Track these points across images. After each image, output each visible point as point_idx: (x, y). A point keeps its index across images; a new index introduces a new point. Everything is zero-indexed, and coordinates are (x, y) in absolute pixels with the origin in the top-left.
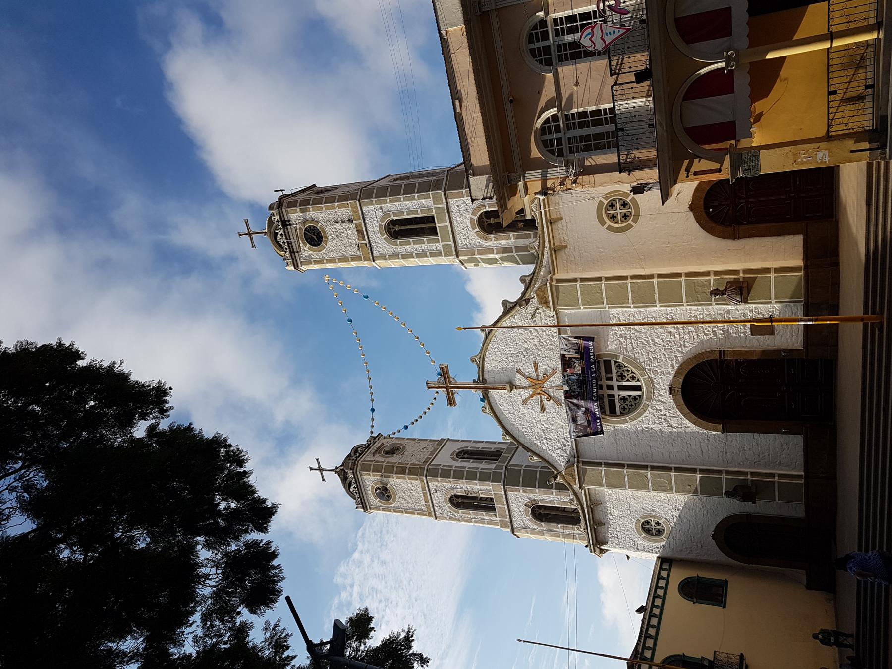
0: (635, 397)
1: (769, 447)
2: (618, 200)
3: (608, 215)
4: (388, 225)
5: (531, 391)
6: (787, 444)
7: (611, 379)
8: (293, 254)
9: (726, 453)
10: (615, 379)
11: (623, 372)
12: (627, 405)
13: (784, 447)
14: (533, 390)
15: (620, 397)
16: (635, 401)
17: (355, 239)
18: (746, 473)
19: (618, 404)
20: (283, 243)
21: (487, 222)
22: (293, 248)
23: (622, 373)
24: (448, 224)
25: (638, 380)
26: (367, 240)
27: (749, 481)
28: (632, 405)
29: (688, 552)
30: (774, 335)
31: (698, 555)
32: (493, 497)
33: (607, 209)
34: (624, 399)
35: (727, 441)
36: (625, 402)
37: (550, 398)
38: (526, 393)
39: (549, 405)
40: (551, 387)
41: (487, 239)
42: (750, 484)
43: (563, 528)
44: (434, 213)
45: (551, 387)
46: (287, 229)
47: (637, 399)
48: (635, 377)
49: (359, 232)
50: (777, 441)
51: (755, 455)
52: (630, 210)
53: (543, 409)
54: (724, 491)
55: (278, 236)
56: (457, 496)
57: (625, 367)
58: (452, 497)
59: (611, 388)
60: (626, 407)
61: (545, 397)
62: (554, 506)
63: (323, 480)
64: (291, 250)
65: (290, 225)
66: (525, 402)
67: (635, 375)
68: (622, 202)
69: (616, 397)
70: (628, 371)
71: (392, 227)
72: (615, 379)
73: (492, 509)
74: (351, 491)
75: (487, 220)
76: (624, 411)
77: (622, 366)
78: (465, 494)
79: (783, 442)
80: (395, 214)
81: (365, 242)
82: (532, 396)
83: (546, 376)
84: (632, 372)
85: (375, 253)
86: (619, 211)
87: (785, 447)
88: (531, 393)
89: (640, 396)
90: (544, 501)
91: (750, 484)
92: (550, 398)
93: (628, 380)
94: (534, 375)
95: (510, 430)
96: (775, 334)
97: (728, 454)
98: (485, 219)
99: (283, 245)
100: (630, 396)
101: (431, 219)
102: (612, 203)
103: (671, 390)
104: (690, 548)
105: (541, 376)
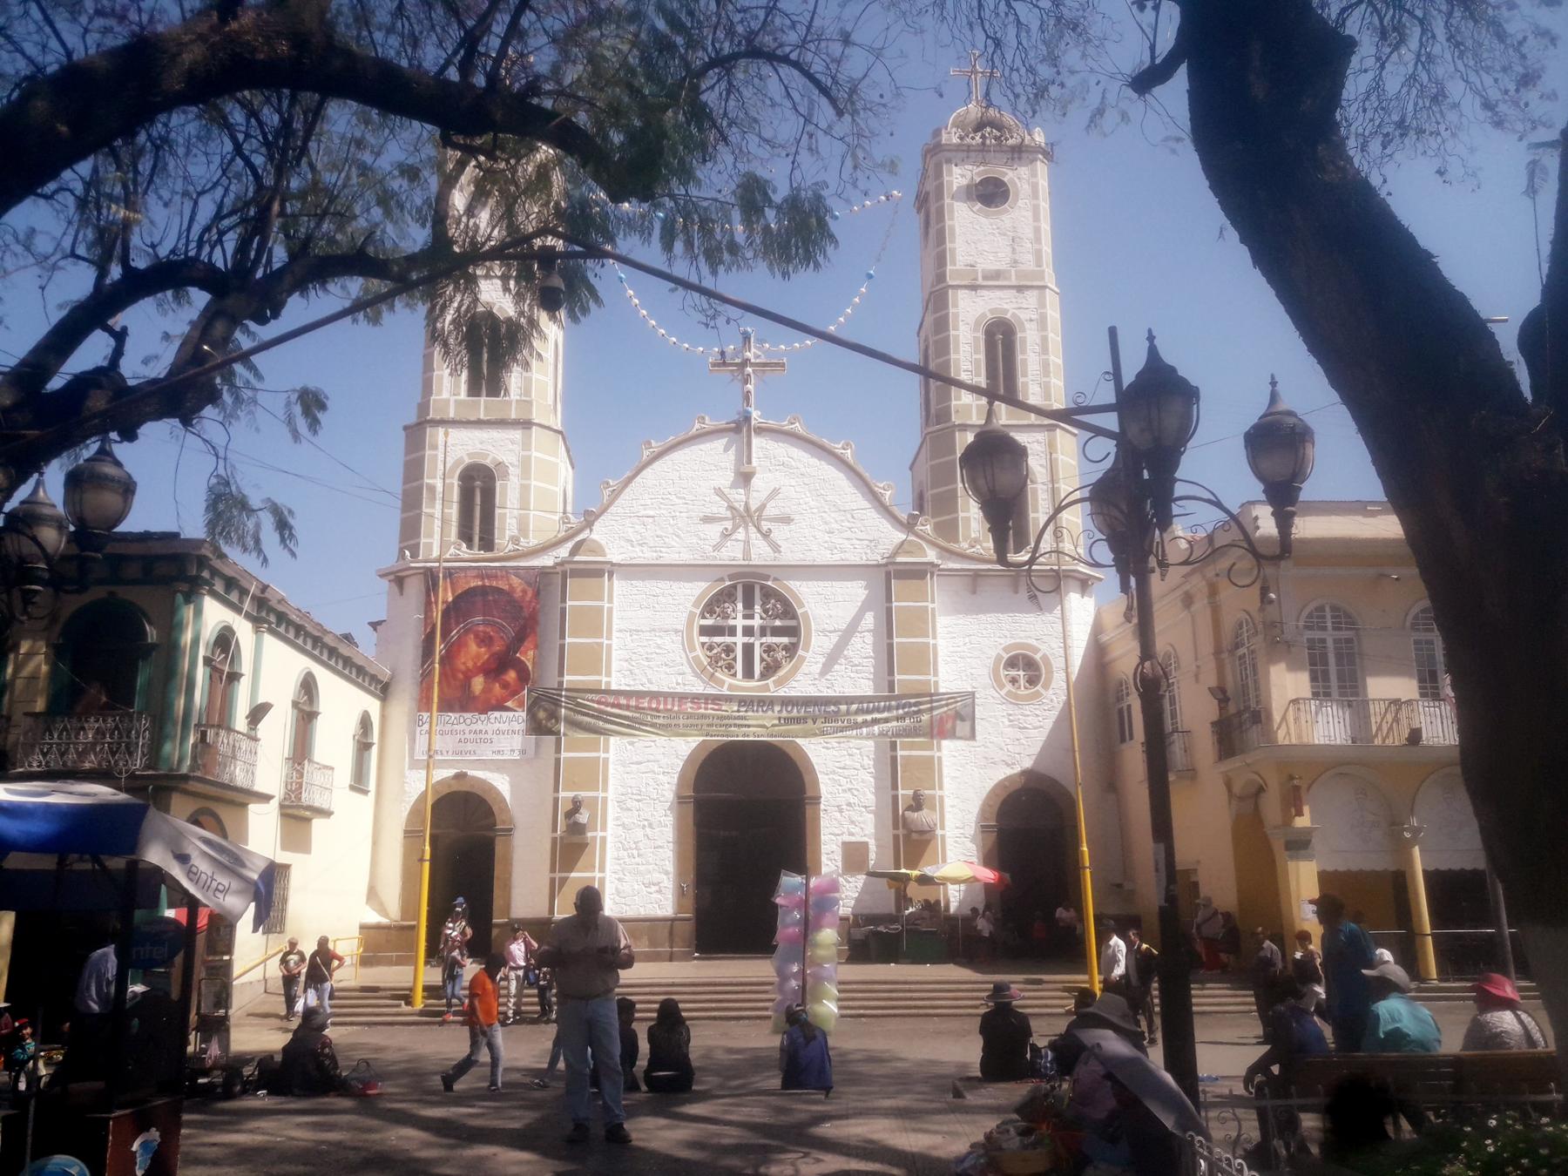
5: (742, 509)
6: (659, 892)
9: (638, 801)
14: (742, 509)
17: (987, 263)
26: (985, 283)
34: (729, 649)
37: (726, 535)
39: (714, 531)
45: (747, 542)
49: (997, 275)
53: (707, 520)
54: (583, 794)
59: (748, 631)
61: (729, 525)
65: (1013, 159)
66: (719, 492)
80: (1024, 340)
81: (980, 278)
83: (766, 535)
87: (654, 888)
88: (736, 505)
89: (734, 675)
90: (504, 487)
92: (726, 535)
93: (762, 660)
100: (735, 659)
105: (765, 526)
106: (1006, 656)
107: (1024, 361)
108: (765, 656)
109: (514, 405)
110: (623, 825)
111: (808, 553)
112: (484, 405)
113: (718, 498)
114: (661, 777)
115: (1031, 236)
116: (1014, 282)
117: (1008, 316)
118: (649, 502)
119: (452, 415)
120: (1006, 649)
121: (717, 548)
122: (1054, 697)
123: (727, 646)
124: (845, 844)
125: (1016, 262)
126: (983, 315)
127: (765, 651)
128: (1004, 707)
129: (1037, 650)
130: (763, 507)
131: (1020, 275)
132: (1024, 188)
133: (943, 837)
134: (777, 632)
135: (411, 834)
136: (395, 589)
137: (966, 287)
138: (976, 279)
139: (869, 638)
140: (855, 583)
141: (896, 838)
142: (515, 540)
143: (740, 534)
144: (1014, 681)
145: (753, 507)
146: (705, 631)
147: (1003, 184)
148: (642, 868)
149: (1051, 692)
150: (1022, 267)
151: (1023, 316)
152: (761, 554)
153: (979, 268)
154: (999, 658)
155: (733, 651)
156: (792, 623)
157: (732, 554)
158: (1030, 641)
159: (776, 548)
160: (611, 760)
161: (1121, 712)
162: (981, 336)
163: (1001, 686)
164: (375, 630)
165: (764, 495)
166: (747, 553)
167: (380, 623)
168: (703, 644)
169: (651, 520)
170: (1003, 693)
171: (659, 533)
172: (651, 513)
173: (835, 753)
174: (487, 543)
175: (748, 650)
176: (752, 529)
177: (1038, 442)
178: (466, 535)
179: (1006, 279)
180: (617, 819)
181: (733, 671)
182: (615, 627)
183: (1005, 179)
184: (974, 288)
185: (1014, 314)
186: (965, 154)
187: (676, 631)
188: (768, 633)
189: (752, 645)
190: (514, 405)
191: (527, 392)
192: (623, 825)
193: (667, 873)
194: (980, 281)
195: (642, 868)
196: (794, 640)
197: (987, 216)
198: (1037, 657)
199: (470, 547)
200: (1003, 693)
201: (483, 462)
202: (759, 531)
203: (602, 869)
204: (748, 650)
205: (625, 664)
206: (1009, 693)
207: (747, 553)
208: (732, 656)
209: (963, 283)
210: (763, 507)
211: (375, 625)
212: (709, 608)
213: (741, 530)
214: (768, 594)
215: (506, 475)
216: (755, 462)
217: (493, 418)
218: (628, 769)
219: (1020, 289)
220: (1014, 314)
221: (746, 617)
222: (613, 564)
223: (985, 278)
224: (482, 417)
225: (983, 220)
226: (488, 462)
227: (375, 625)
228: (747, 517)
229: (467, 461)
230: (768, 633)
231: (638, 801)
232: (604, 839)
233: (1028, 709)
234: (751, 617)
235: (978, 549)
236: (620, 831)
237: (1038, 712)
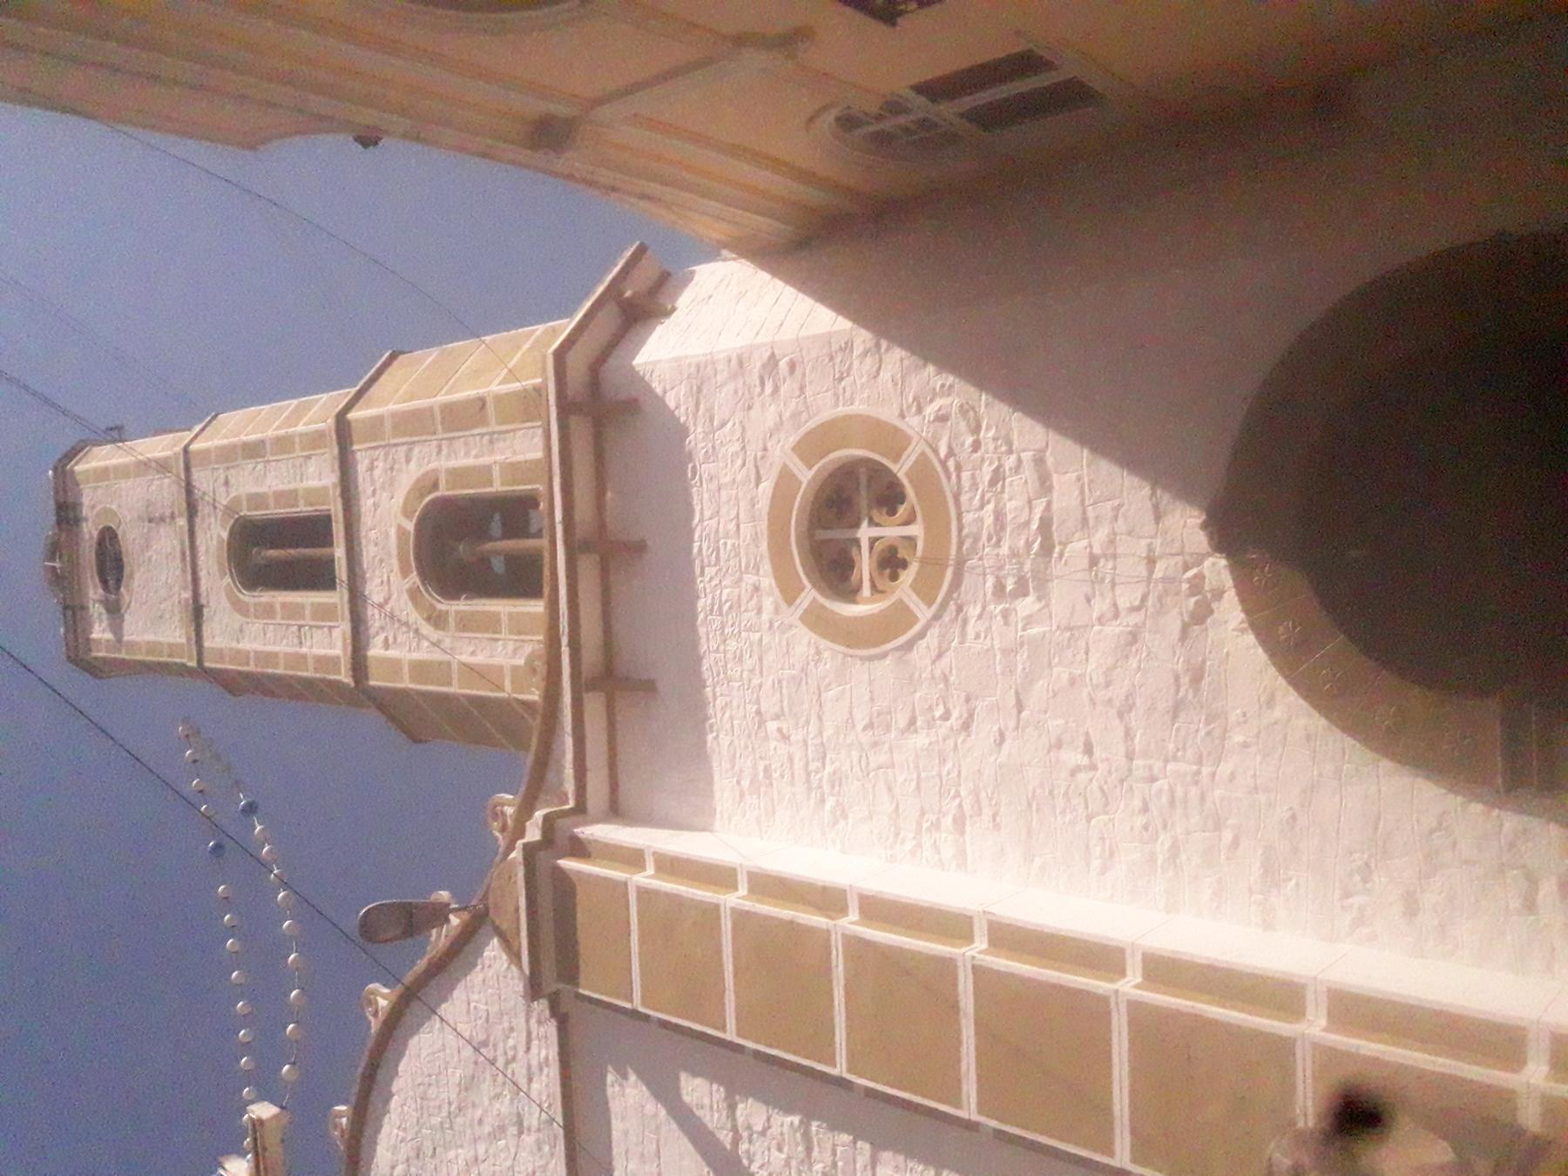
106: (810, 595)
120: (789, 593)
122: (930, 410)
128: (973, 611)
129: (786, 479)
139: (751, 1112)
140: (615, 1106)
144: (891, 562)
149: (912, 424)
154: (817, 621)
158: (764, 505)
170: (924, 613)
197: (131, 576)
198: (806, 476)
200: (924, 613)
206: (926, 590)
225: (137, 582)
233: (977, 516)
237: (986, 473)
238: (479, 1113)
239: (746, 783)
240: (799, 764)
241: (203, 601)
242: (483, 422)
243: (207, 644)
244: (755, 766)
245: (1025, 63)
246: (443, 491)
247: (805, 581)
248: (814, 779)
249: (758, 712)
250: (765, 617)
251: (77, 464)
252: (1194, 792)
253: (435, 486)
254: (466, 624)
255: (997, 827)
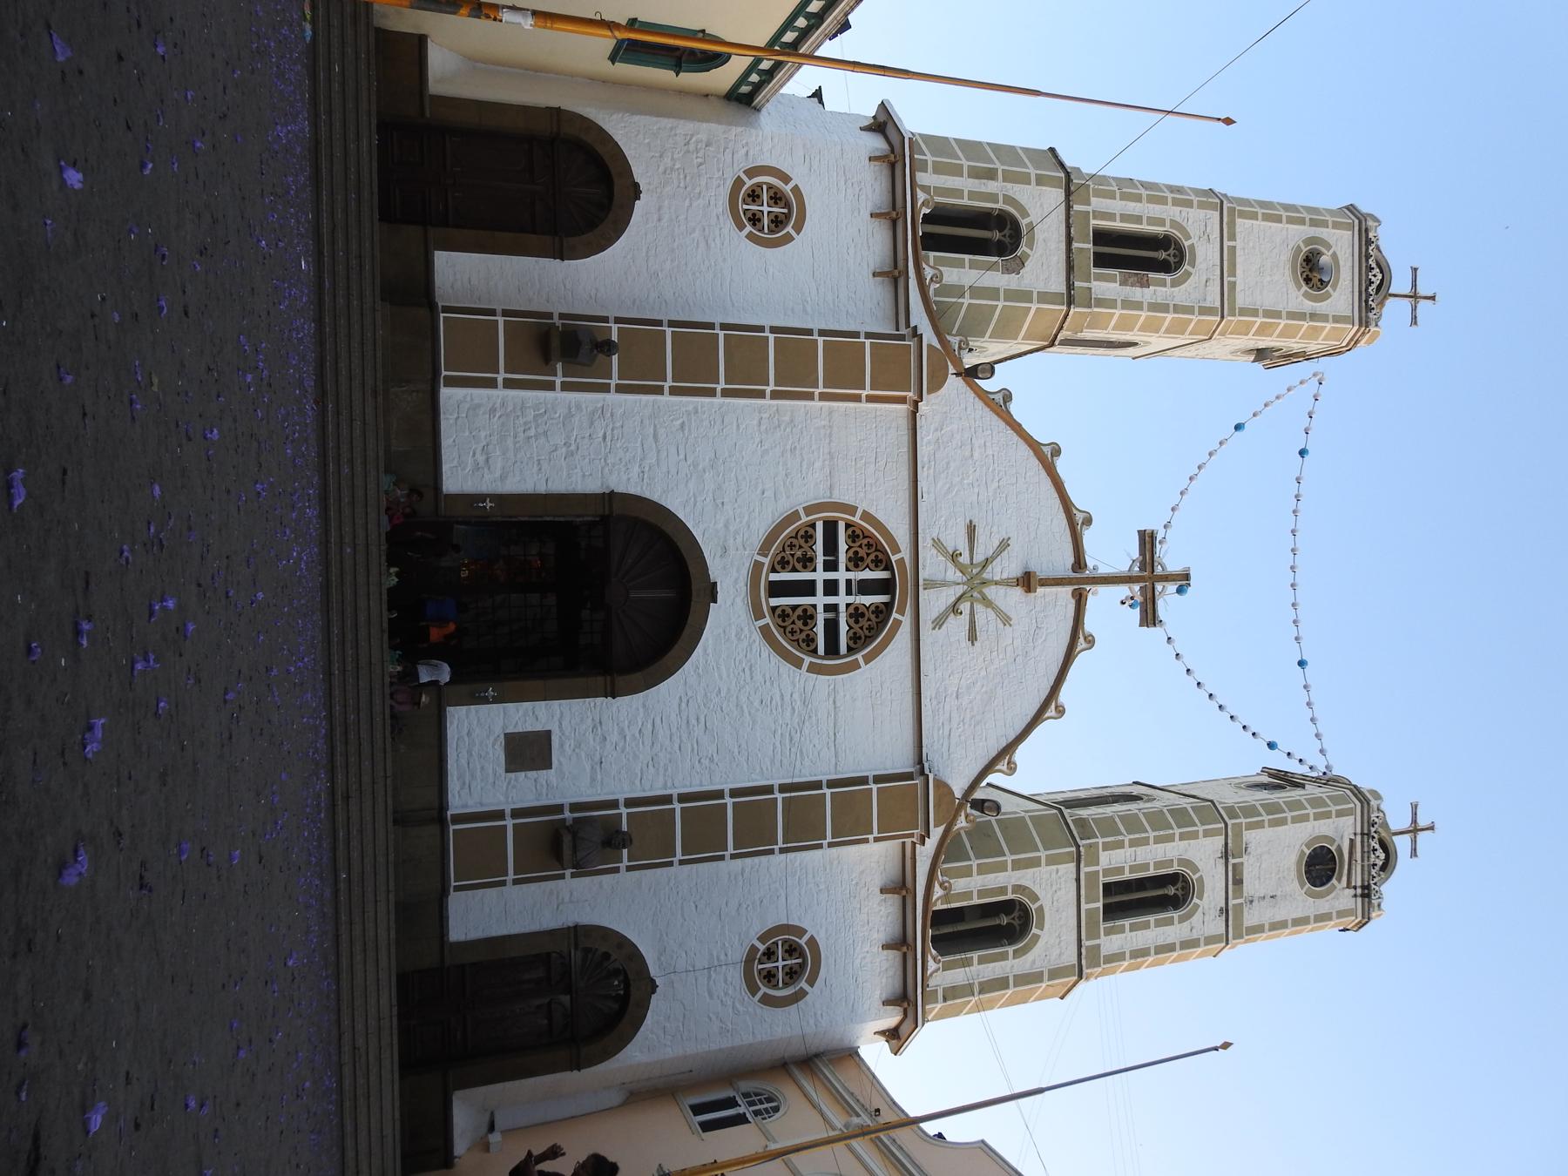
0: (783, 568)
1: (515, 456)
2: (781, 985)
3: (802, 955)
4: (1185, 901)
5: (985, 575)
6: (477, 467)
7: (829, 608)
8: (1366, 832)
9: (604, 438)
10: (820, 609)
11: (803, 628)
12: (800, 547)
13: (484, 457)
15: (813, 567)
16: (783, 558)
18: (566, 387)
19: (819, 547)
20: (1376, 850)
21: (1013, 919)
22: (1362, 842)
23: (805, 624)
24: (1084, 907)
25: (774, 609)
26: (1230, 868)
27: (560, 372)
28: (792, 546)
29: (694, 139)
30: (505, 734)
31: (671, 129)
32: (1094, 270)
33: (803, 966)
34: (807, 562)
35: (603, 468)
36: (804, 555)
37: (954, 557)
38: (998, 571)
40: (944, 584)
41: (1018, 888)
42: (559, 366)
43: (958, 193)
44: (1102, 927)
45: (944, 584)
46: (1363, 880)
47: (778, 563)
48: (779, 616)
49: (1238, 882)
50: (498, 474)
51: (545, 433)
52: (761, 967)
53: (971, 530)
54: (615, 358)
55: (1381, 863)
56: (1165, 267)
57: (798, 640)
58: (1179, 264)
59: (831, 588)
60: (802, 542)
61: (965, 559)
62: (971, 257)
63: (1415, 270)
64: (1366, 840)
66: (1004, 545)
67: (780, 621)
68: (774, 981)
69: (820, 566)
70: (793, 632)
71: (1180, 893)
72: (820, 609)
73: (1101, 237)
74: (1382, 272)
75: (1012, 921)
76: (806, 532)
77: (803, 641)
78: (1152, 275)
79: (486, 470)
80: (1170, 922)
82: (987, 562)
83: (954, 609)
84: (785, 628)
85: (1220, 840)
86: (780, 964)
87: (481, 458)
88: (989, 569)
90: (991, 267)
91: (559, 366)
92: (954, 557)
93: (794, 608)
94: (979, 608)
95: (1043, 474)
96: (502, 736)
97: (601, 435)
98: (1016, 923)
99: (1377, 846)
100: (794, 570)
101: (1111, 911)
102: (791, 978)
103: (712, 593)
104: (689, 152)
105: (965, 607)
106: (803, 942)
107: (1146, 926)
108: (799, 612)
109: (1086, 285)
110: (569, 415)
111: (932, 667)
112: (1085, 246)
113: (997, 543)
114: (636, 469)
115: (1278, 918)
116: (1232, 902)
117: (1195, 900)
118: (990, 452)
119: (1076, 207)
121: (937, 544)
123: (811, 560)
124: (548, 733)
125: (1251, 902)
126: (1196, 869)
127: (805, 611)
130: (988, 603)
131: (1239, 907)
132: (1324, 906)
133: (562, 877)
134: (832, 627)
135: (557, 113)
136: (866, 123)
137: (1226, 844)
138: (1234, 857)
141: (558, 809)
142: (937, 278)
143: (953, 574)
145: (990, 592)
146: (831, 527)
147: (1329, 879)
148: (510, 442)
150: (1245, 910)
151: (1197, 917)
152: (933, 602)
153: (1244, 859)
154: (801, 932)
155: (805, 567)
156: (843, 649)
157: (932, 565)
159: (939, 622)
160: (659, 397)
161: (731, 1103)
162: (1175, 868)
163: (762, 939)
164: (813, 95)
165: (1000, 603)
166: (931, 584)
167: (821, 101)
168: (813, 526)
169: (967, 453)
171: (952, 465)
172: (976, 455)
173: (673, 716)
174: (931, 242)
175: (808, 588)
176: (960, 590)
177: (1060, 954)
178: (939, 216)
179: (1234, 891)
180: (578, 407)
181: (778, 567)
182: (835, 404)
183: (1334, 881)
184: (1226, 855)
185: (1197, 906)
186: (1359, 831)
187: (831, 488)
188: (830, 615)
189: (813, 594)
190: (1086, 285)
191: (1101, 303)
192: (569, 415)
193: (503, 478)
194: (1232, 861)
195: (510, 442)
196: (821, 650)
199: (927, 219)
201: (1024, 241)
202: (959, 599)
203: (509, 384)
204: (808, 588)
205: (787, 418)
207: (931, 584)
208: (799, 566)
209: (1229, 841)
210: (988, 603)
211: (818, 95)
212: (854, 535)
213: (959, 574)
214: (883, 612)
215: (1007, 270)
216: (1040, 590)
217: (1074, 256)
218: (647, 422)
219: (1225, 911)
220: (1197, 906)
221: (849, 582)
222: (916, 404)
223: (1234, 865)
224: (1075, 245)
225: (1294, 858)
226: (1023, 248)
227: (818, 95)
228: (976, 583)
229: (1024, 222)
230: (830, 615)
231: (604, 438)
232: (550, 386)
234: (849, 592)
235: (938, 892)
236: (561, 411)
238: (984, 689)
239: (836, 862)
240: (810, 876)
241: (1223, 861)
242: (980, 983)
243: (1223, 837)
244: (831, 869)
245: (707, 1127)
246: (1010, 949)
247: (805, 947)
248: (804, 871)
249: (828, 891)
250: (824, 928)
251: (1354, 921)
252: (662, 901)
253: (1015, 952)
254: (1003, 890)
255: (729, 874)
